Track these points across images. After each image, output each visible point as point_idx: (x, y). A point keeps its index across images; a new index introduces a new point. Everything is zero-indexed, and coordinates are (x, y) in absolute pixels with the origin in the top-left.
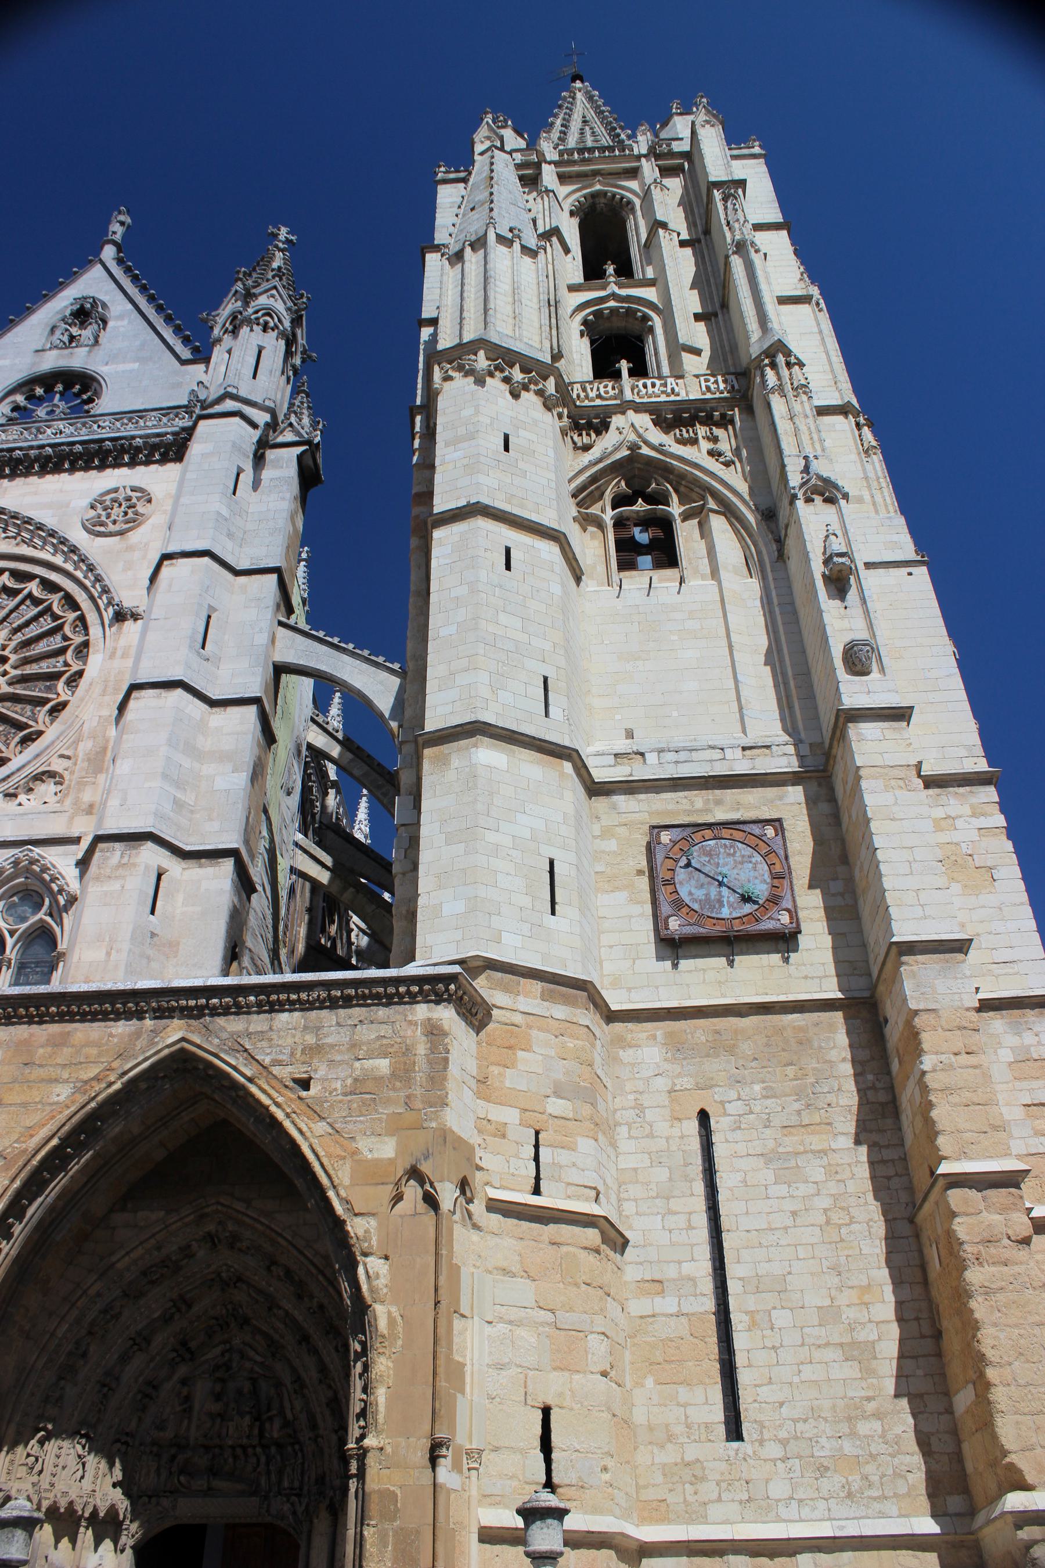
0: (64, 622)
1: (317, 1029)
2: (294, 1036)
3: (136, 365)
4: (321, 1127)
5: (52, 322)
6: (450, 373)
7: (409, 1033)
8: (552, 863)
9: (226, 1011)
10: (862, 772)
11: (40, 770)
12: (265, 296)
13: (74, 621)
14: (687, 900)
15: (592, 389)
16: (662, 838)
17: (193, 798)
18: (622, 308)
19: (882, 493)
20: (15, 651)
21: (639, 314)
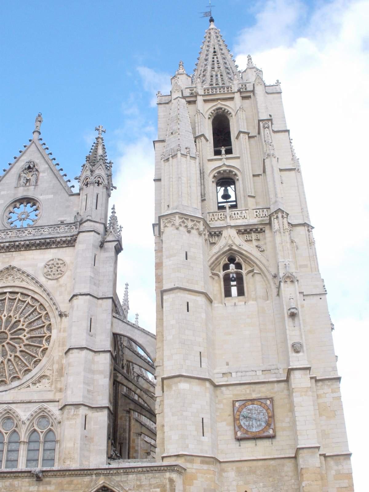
0: (42, 316)
1: (140, 480)
2: (134, 482)
3: (51, 196)
5: (19, 172)
6: (167, 225)
7: (165, 481)
8: (203, 419)
9: (115, 474)
10: (294, 390)
11: (42, 375)
12: (97, 170)
13: (45, 315)
14: (243, 426)
15: (216, 215)
16: (236, 405)
17: (93, 387)
18: (228, 170)
19: (314, 262)
20: (27, 327)
21: (234, 173)
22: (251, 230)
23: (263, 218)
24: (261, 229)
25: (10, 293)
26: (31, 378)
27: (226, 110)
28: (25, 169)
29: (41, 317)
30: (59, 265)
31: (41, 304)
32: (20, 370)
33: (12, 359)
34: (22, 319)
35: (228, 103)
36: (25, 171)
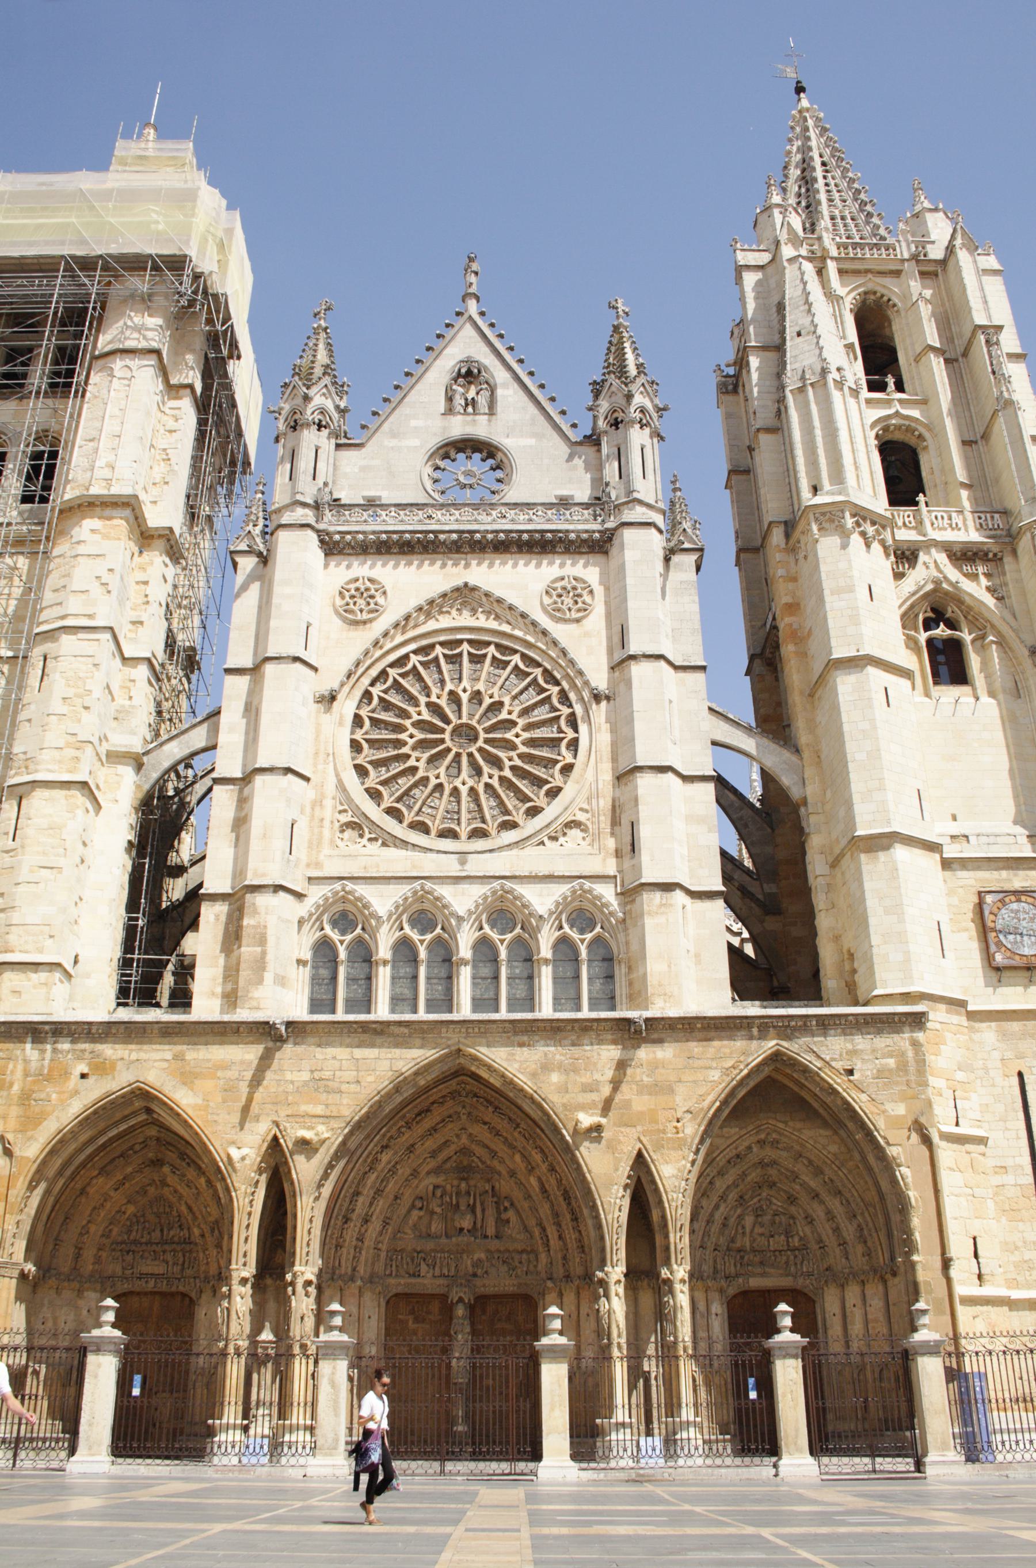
3: (532, 441)
4: (864, 1097)
22: (975, 554)
23: (992, 533)
24: (995, 555)
25: (470, 642)
26: (548, 826)
27: (885, 299)
28: (459, 375)
29: (549, 697)
30: (579, 591)
31: (546, 671)
32: (517, 810)
33: (495, 782)
34: (507, 700)
35: (888, 281)
36: (461, 380)
